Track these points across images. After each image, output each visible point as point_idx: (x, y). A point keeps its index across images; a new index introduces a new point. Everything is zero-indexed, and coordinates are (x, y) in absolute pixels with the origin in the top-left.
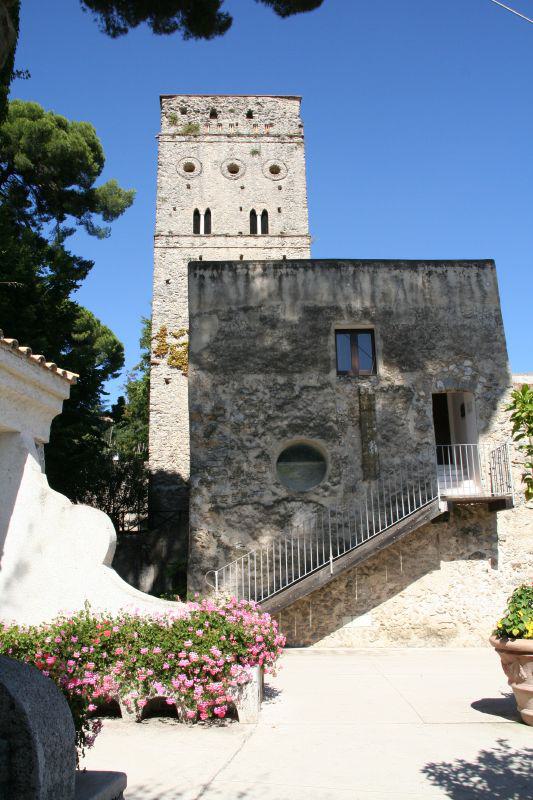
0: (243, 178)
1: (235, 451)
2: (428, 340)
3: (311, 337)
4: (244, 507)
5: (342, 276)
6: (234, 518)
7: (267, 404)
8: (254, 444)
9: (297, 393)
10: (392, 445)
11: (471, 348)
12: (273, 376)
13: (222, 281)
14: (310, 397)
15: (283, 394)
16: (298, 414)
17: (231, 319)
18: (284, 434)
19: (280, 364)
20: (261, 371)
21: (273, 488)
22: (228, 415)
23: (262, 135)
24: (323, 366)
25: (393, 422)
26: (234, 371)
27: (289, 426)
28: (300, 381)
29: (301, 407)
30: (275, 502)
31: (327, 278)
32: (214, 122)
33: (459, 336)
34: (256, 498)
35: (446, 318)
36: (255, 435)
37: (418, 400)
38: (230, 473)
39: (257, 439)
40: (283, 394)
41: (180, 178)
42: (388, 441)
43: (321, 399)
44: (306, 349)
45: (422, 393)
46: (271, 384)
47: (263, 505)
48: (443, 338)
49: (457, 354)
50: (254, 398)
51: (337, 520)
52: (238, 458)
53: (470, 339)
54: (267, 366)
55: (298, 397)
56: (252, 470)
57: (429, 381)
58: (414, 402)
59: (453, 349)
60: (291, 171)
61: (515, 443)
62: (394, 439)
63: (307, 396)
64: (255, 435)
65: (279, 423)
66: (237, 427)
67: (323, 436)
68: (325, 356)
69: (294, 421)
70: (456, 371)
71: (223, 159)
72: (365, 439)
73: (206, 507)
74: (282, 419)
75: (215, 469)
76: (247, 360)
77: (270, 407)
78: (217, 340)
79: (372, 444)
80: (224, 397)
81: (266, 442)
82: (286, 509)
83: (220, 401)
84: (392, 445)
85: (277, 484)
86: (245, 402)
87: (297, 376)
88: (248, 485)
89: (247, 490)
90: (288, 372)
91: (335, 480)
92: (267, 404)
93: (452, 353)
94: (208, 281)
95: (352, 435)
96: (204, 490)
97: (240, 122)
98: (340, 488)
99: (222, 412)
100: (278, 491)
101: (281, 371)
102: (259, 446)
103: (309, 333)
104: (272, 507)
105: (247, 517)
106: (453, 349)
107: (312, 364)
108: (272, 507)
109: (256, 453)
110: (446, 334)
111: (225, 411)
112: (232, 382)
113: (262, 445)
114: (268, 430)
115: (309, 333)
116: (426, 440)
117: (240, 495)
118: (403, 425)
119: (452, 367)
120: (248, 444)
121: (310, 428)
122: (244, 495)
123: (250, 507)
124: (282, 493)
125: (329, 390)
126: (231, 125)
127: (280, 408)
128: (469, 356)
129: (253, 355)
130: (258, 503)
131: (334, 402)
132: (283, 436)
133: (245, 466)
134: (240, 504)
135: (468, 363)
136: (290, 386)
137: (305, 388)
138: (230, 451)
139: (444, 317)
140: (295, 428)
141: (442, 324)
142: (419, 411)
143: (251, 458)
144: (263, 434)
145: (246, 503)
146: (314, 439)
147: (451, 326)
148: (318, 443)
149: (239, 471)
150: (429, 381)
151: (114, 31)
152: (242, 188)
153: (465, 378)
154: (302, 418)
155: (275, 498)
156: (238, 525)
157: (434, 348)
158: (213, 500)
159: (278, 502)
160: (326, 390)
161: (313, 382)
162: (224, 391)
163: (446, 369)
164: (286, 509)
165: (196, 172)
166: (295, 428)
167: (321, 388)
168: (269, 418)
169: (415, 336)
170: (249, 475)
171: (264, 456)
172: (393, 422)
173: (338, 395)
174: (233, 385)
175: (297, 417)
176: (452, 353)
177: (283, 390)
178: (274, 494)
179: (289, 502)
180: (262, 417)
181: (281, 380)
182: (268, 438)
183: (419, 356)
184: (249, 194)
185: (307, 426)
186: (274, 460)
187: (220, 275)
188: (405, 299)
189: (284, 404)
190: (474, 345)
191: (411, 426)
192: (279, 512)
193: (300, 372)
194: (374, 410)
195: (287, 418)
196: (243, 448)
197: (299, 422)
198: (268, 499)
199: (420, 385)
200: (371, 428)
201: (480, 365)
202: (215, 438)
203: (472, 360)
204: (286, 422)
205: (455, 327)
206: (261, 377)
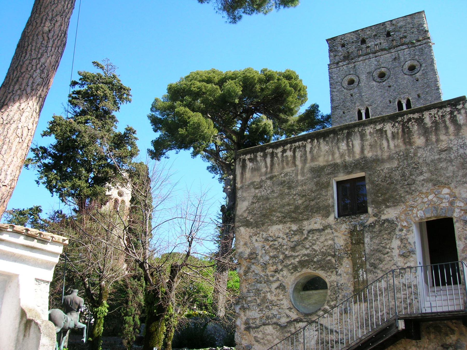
0: (389, 80)
1: (263, 285)
2: (409, 177)
3: (316, 190)
4: (266, 327)
5: (338, 138)
6: (260, 336)
7: (285, 247)
8: (275, 278)
9: (306, 236)
10: (379, 271)
11: (448, 177)
12: (288, 225)
13: (257, 161)
14: (315, 238)
15: (296, 238)
16: (306, 252)
17: (261, 187)
18: (295, 268)
19: (293, 215)
20: (281, 222)
21: (287, 311)
22: (259, 257)
23: (399, 46)
24: (324, 212)
25: (380, 251)
26: (263, 224)
27: (300, 262)
28: (308, 225)
29: (308, 246)
30: (288, 322)
31: (327, 142)
32: (364, 46)
33: (436, 169)
34: (275, 320)
35: (424, 155)
36: (276, 271)
37: (401, 230)
38: (259, 301)
39: (277, 274)
40: (296, 238)
41: (345, 91)
42: (375, 268)
43: (322, 239)
44: (313, 200)
45: (405, 224)
46: (288, 231)
47: (280, 325)
48: (421, 173)
49: (434, 185)
50: (276, 243)
51: (333, 337)
52: (264, 290)
53: (446, 168)
54: (285, 218)
55: (306, 238)
56: (274, 298)
57: (410, 213)
58: (397, 232)
59: (431, 180)
60: (424, 65)
61: (158, 236)
62: (381, 266)
63: (313, 237)
64: (276, 271)
65: (293, 261)
66: (265, 266)
67: (323, 268)
68: (326, 204)
69: (303, 258)
70: (435, 199)
71: (373, 70)
72: (356, 268)
73: (243, 327)
74: (295, 257)
75: (249, 299)
76: (271, 215)
77: (286, 249)
78: (253, 203)
79: (361, 272)
80: (256, 245)
81: (283, 277)
82: (295, 328)
83: (254, 248)
84: (379, 271)
85: (290, 309)
86: (270, 246)
87: (305, 223)
88: (270, 309)
89: (269, 313)
90: (299, 220)
91: (332, 303)
92: (285, 247)
93: (430, 185)
94: (248, 162)
95: (346, 266)
96: (242, 314)
97: (382, 41)
98: (337, 310)
99: (254, 256)
100: (291, 314)
101: (294, 220)
102: (278, 280)
103: (315, 188)
104: (285, 327)
105: (268, 334)
106: (431, 180)
107: (316, 211)
108: (285, 327)
109: (275, 285)
110: (425, 169)
111: (257, 255)
112: (261, 233)
113: (280, 278)
114: (285, 266)
115: (315, 188)
116: (408, 264)
117: (265, 318)
118: (388, 253)
119: (430, 197)
120: (271, 279)
121: (315, 262)
122: (268, 318)
123: (270, 327)
124: (294, 315)
125: (329, 231)
126: (376, 45)
127: (293, 249)
128: (446, 185)
129: (275, 211)
130: (276, 324)
131: (333, 240)
132: (295, 271)
133: (269, 296)
134: (264, 324)
135: (445, 191)
136: (300, 231)
137: (311, 231)
138: (259, 285)
139: (422, 155)
140: (303, 264)
141: (421, 161)
142: (401, 240)
143: (273, 289)
144: (281, 270)
145: (268, 324)
146: (317, 271)
147: (428, 161)
148: (321, 274)
149: (264, 300)
150: (410, 213)
151: (295, 6)
152: (390, 87)
153: (443, 205)
154: (307, 255)
155: (288, 320)
156: (262, 341)
157: (414, 183)
158: (247, 323)
159: (290, 323)
160: (326, 231)
161: (317, 226)
162: (256, 240)
163: (426, 200)
164: (295, 328)
165: (356, 84)
166: (303, 264)
167: (323, 230)
168: (286, 257)
169: (397, 175)
170: (271, 302)
171: (282, 287)
172: (380, 251)
173: (336, 234)
174: (263, 235)
175: (305, 255)
176: (430, 185)
177: (295, 235)
178: (288, 316)
179: (298, 322)
180: (281, 257)
181: (294, 227)
182: (285, 272)
183: (401, 192)
184: (394, 90)
185: (312, 261)
186: (290, 289)
187: (256, 157)
188: (389, 146)
189: (296, 246)
190: (451, 174)
191: (396, 252)
192: (290, 331)
193: (308, 219)
194: (363, 243)
195: (298, 256)
196: (268, 282)
197: (307, 258)
198: (284, 321)
199: (403, 217)
200: (360, 258)
201: (457, 191)
202: (250, 275)
203: (449, 188)
204: (297, 260)
205: (432, 161)
206: (280, 226)
